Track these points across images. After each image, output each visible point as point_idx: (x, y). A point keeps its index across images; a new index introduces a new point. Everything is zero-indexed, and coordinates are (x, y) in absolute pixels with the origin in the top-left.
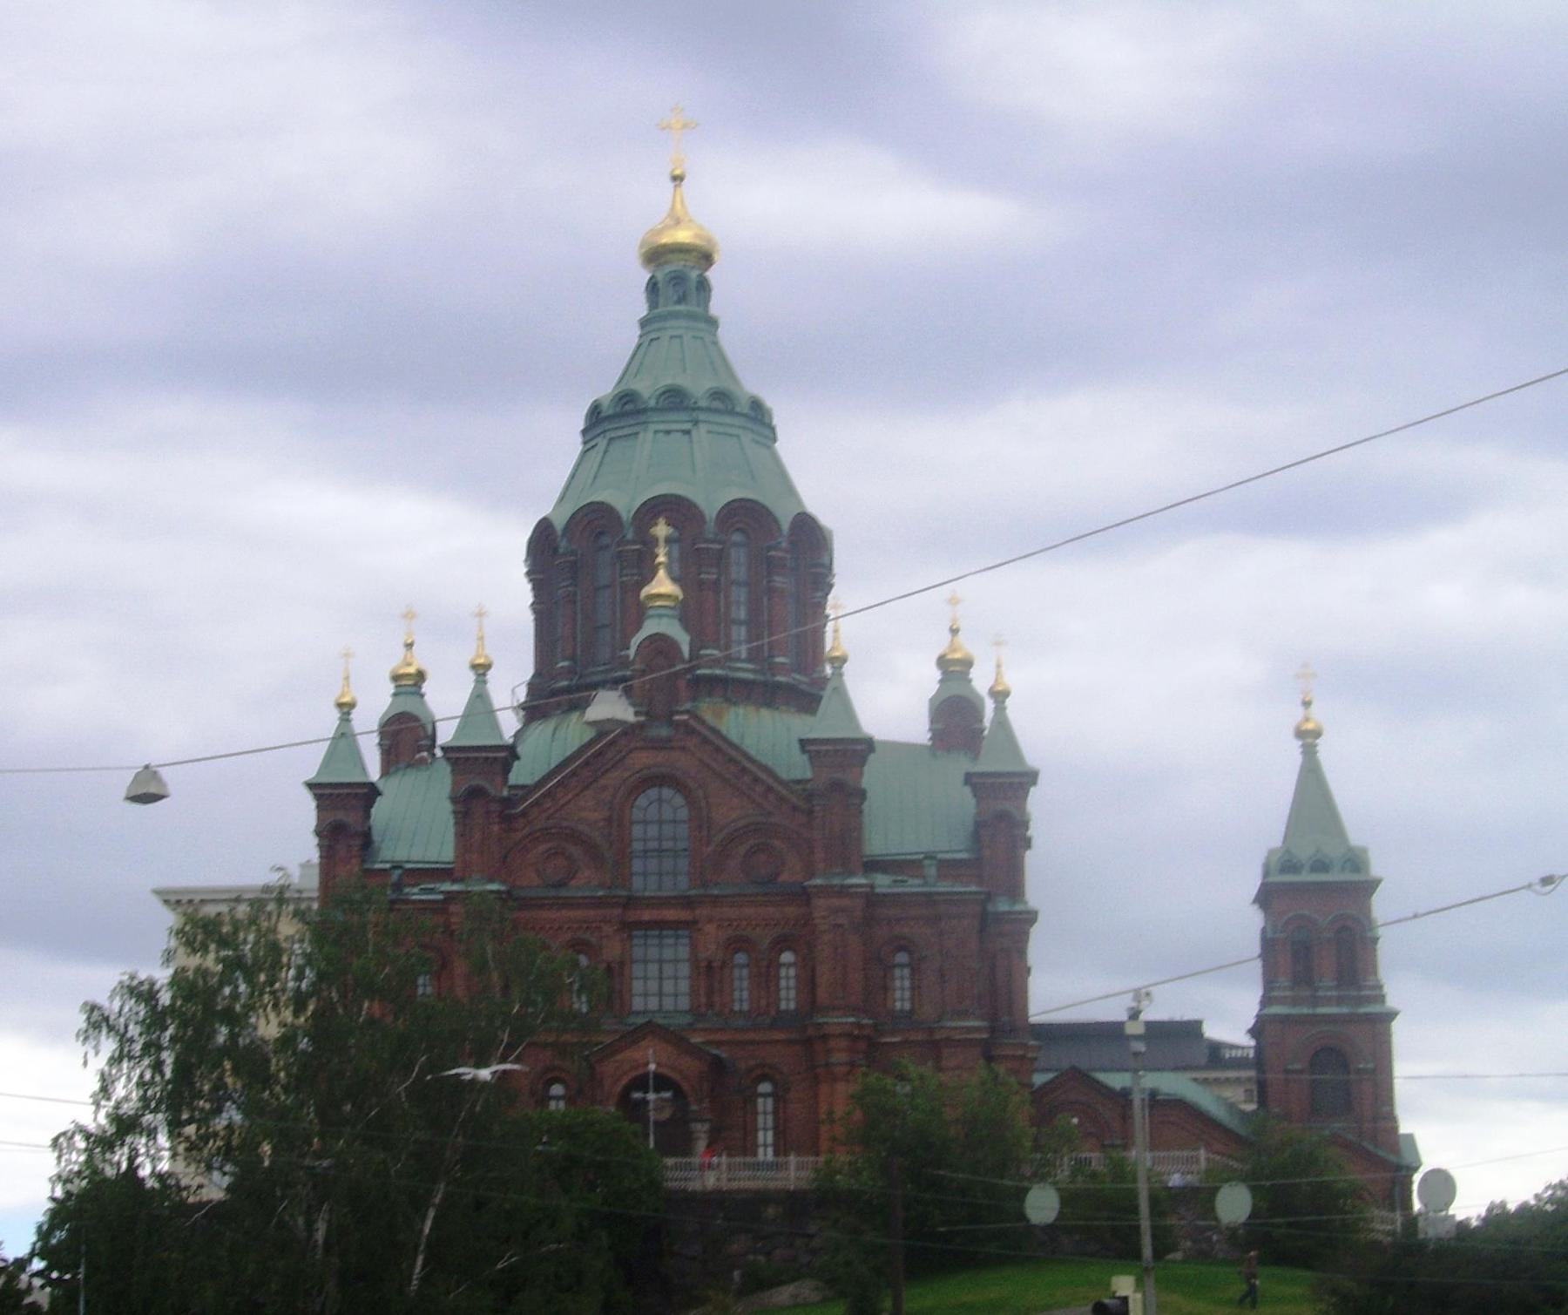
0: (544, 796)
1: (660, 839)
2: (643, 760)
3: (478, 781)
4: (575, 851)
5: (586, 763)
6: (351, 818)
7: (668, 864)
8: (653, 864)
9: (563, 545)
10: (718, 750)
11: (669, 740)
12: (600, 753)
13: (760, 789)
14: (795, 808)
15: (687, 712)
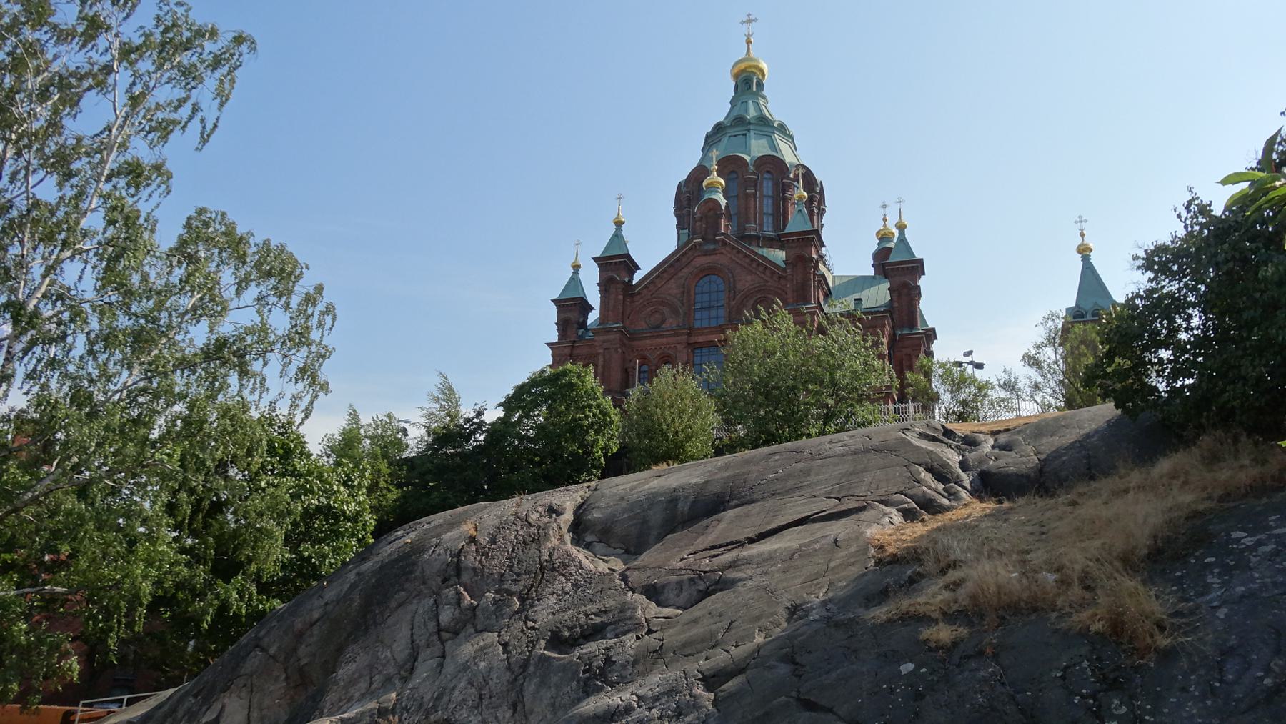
0: (649, 283)
1: (710, 301)
2: (702, 261)
3: (611, 274)
4: (665, 310)
5: (671, 265)
6: (573, 316)
7: (713, 313)
8: (705, 314)
9: (684, 190)
10: (739, 252)
11: (714, 250)
12: (678, 260)
13: (761, 269)
14: (780, 277)
15: (723, 234)
